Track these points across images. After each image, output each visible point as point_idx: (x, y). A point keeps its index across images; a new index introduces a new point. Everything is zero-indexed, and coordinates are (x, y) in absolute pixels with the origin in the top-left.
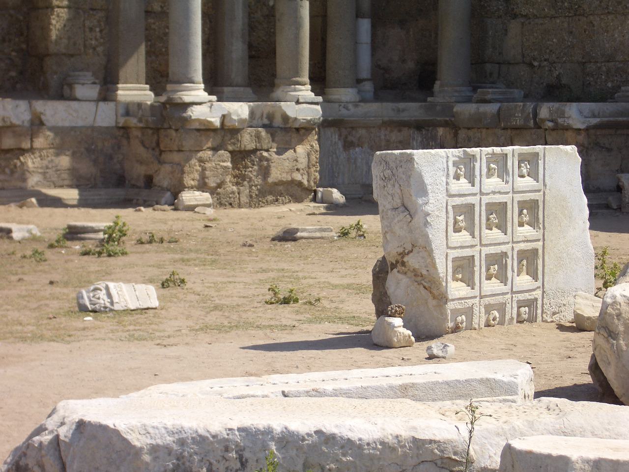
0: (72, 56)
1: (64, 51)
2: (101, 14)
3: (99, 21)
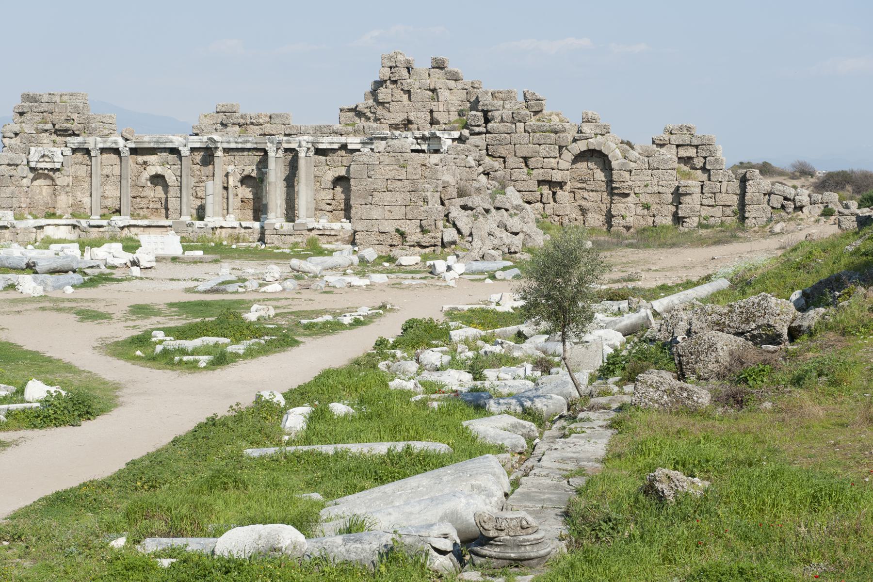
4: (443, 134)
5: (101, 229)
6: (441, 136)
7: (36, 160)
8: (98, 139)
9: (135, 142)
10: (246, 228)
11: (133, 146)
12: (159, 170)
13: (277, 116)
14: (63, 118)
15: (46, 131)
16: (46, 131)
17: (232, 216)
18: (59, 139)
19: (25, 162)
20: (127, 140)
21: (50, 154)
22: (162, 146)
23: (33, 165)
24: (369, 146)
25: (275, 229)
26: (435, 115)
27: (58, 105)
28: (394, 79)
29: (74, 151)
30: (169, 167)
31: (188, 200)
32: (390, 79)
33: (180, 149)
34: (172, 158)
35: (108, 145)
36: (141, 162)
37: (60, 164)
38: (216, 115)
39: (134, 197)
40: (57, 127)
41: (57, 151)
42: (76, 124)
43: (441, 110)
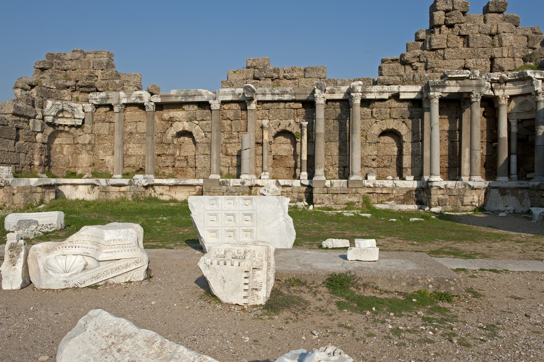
4: (535, 73)
5: (123, 189)
6: (532, 76)
7: (53, 114)
8: (122, 94)
9: (161, 96)
11: (159, 100)
12: (186, 126)
13: (312, 69)
14: (86, 74)
15: (68, 87)
16: (68, 87)
17: (267, 173)
18: (82, 96)
19: (39, 116)
20: (152, 94)
21: (69, 110)
22: (190, 100)
24: (440, 90)
25: (326, 187)
26: (498, 61)
27: (81, 61)
28: (452, 22)
29: (97, 106)
30: (197, 122)
31: (219, 157)
32: (445, 24)
35: (133, 100)
36: (167, 118)
37: (81, 121)
38: (246, 70)
39: (159, 155)
40: (79, 83)
41: (79, 107)
42: (99, 80)
43: (505, 55)
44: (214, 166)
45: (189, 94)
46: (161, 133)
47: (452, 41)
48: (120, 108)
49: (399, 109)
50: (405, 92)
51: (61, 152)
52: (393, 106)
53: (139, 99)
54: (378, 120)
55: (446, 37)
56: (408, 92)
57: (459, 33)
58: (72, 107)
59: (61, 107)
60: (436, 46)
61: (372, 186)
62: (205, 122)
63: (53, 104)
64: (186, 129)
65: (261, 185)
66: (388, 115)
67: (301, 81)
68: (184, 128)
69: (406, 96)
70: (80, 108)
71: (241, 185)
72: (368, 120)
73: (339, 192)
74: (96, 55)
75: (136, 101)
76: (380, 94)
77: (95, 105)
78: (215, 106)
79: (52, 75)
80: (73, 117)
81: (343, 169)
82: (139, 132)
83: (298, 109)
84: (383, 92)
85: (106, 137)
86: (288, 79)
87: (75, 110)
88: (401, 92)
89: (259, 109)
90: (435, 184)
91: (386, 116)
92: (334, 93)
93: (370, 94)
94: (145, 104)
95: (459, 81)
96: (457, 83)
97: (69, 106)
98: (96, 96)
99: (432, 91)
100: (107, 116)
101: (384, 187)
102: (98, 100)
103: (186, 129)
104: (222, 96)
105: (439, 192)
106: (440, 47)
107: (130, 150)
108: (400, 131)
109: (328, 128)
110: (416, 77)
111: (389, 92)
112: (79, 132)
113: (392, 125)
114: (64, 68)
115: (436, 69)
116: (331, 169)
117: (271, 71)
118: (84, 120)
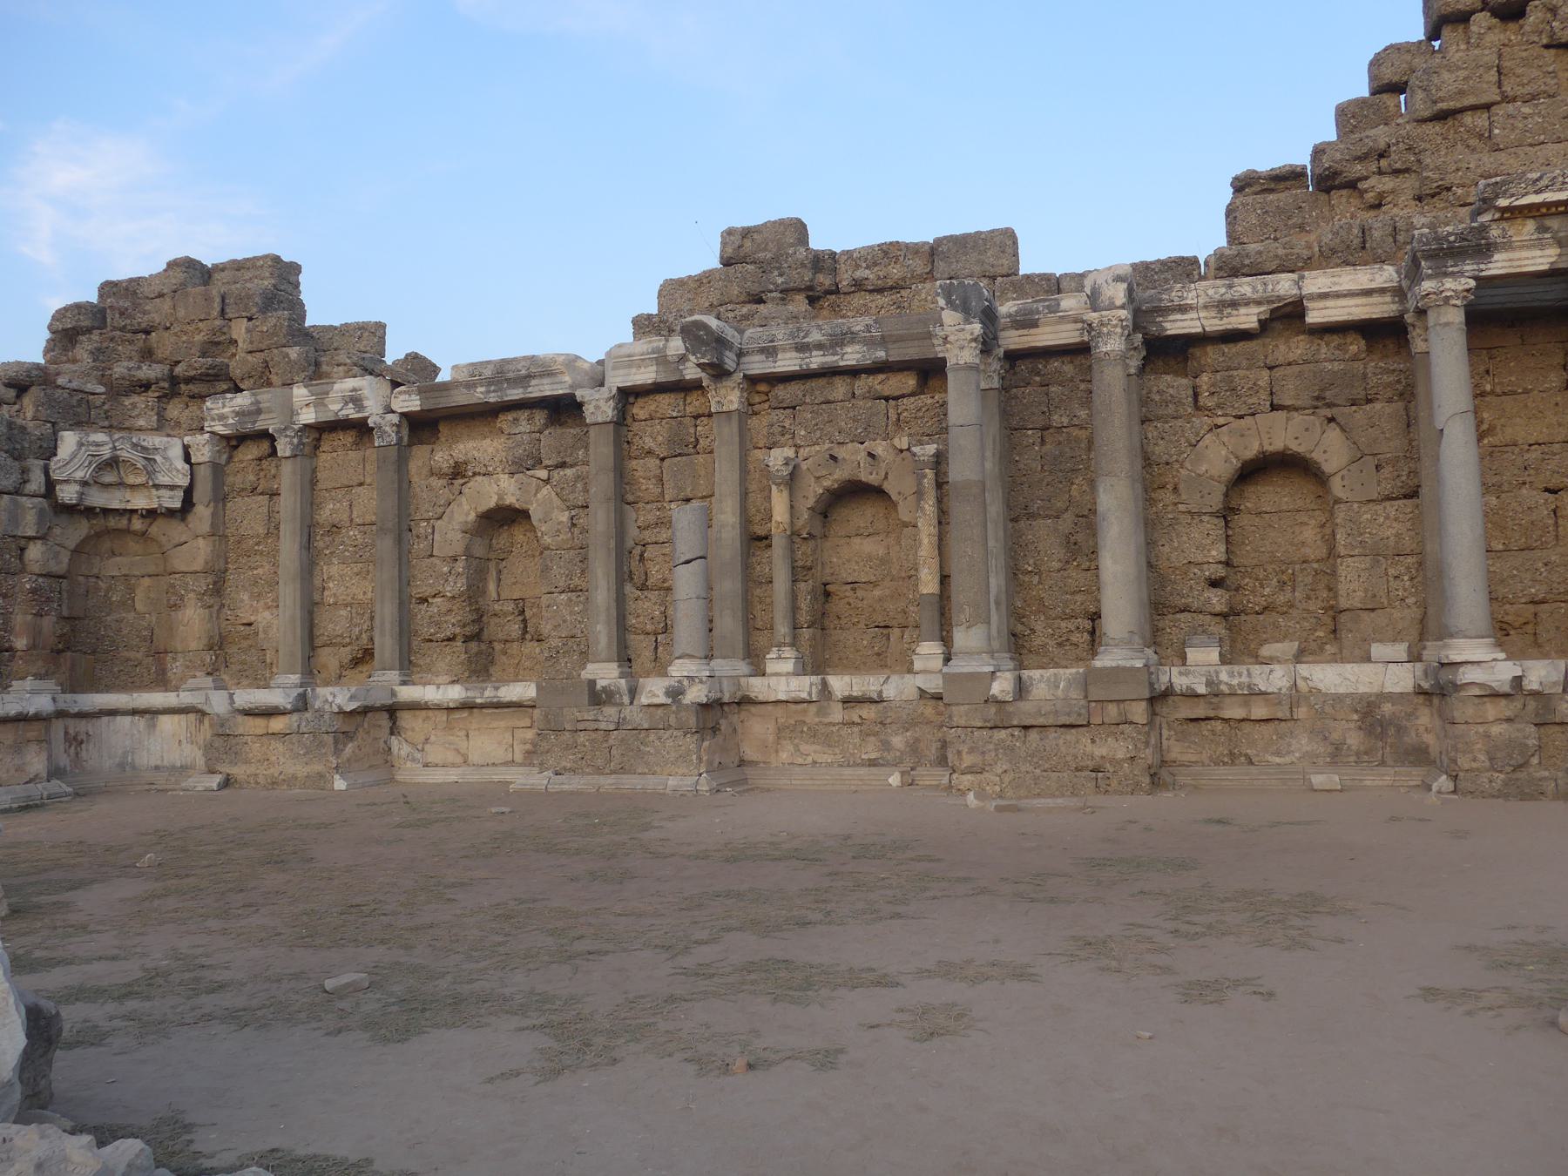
0: (1373, 610)
1: (1359, 605)
2: (1410, 560)
3: (1408, 568)
5: (277, 724)
7: (79, 475)
10: (848, 701)
14: (198, 338)
16: (145, 386)
19: (36, 483)
22: (515, 394)
23: (67, 494)
24: (1469, 267)
30: (543, 474)
33: (579, 394)
34: (553, 440)
37: (181, 494)
42: (241, 355)
44: (602, 633)
45: (511, 375)
46: (428, 520)
47: (1519, 71)
48: (295, 441)
49: (1306, 367)
50: (1324, 296)
51: (128, 603)
52: (1281, 360)
53: (351, 405)
54: (1221, 421)
55: (1495, 57)
56: (1338, 295)
57: (1552, 34)
58: (145, 449)
59: (106, 452)
60: (1451, 98)
61: (1202, 690)
62: (569, 472)
63: (80, 444)
64: (507, 503)
65: (761, 698)
66: (1264, 395)
67: (918, 292)
68: (501, 497)
69: (1334, 312)
70: (176, 452)
71: (669, 701)
72: (1179, 422)
73: (1051, 721)
74: (239, 274)
75: (344, 412)
76: (1220, 312)
77: (227, 438)
78: (597, 407)
79: (98, 349)
80: (151, 484)
81: (1088, 625)
82: (359, 521)
83: (903, 396)
84: (1234, 304)
85: (258, 544)
86: (871, 291)
87: (158, 458)
88: (1312, 297)
89: (756, 408)
90: (1468, 675)
91: (1254, 400)
92: (1034, 324)
93: (1179, 316)
94: (370, 422)
95: (1549, 222)
96: (1542, 229)
97: (135, 446)
98: (224, 406)
99: (1430, 277)
100: (262, 474)
101: (1255, 694)
102: (231, 421)
103: (510, 500)
104: (622, 372)
105: (1492, 710)
106: (1470, 100)
107: (331, 585)
108: (1316, 456)
109: (1021, 466)
110: (1376, 234)
111: (1258, 303)
112: (176, 531)
113: (1280, 435)
114: (139, 323)
115: (1460, 191)
116: (1039, 627)
117: (803, 265)
118: (189, 492)
